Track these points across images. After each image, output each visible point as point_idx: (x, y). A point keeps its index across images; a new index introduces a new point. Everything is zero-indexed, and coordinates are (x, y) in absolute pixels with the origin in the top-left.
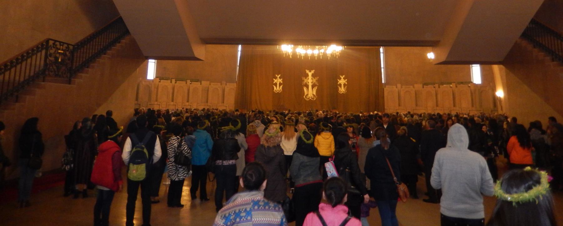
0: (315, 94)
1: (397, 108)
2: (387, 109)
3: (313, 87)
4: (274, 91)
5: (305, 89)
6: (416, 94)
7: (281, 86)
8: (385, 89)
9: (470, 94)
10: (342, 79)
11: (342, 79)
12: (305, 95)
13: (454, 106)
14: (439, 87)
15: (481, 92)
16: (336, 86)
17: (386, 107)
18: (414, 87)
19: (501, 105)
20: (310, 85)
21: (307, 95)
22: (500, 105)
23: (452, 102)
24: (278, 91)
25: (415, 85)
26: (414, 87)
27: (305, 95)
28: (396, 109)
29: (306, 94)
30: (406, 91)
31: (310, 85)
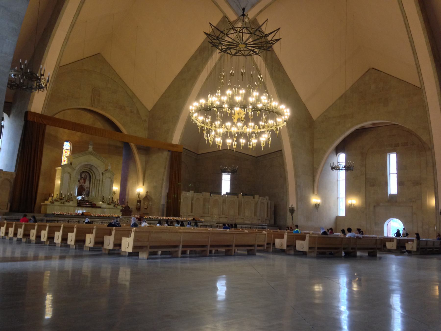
13: (239, 214)
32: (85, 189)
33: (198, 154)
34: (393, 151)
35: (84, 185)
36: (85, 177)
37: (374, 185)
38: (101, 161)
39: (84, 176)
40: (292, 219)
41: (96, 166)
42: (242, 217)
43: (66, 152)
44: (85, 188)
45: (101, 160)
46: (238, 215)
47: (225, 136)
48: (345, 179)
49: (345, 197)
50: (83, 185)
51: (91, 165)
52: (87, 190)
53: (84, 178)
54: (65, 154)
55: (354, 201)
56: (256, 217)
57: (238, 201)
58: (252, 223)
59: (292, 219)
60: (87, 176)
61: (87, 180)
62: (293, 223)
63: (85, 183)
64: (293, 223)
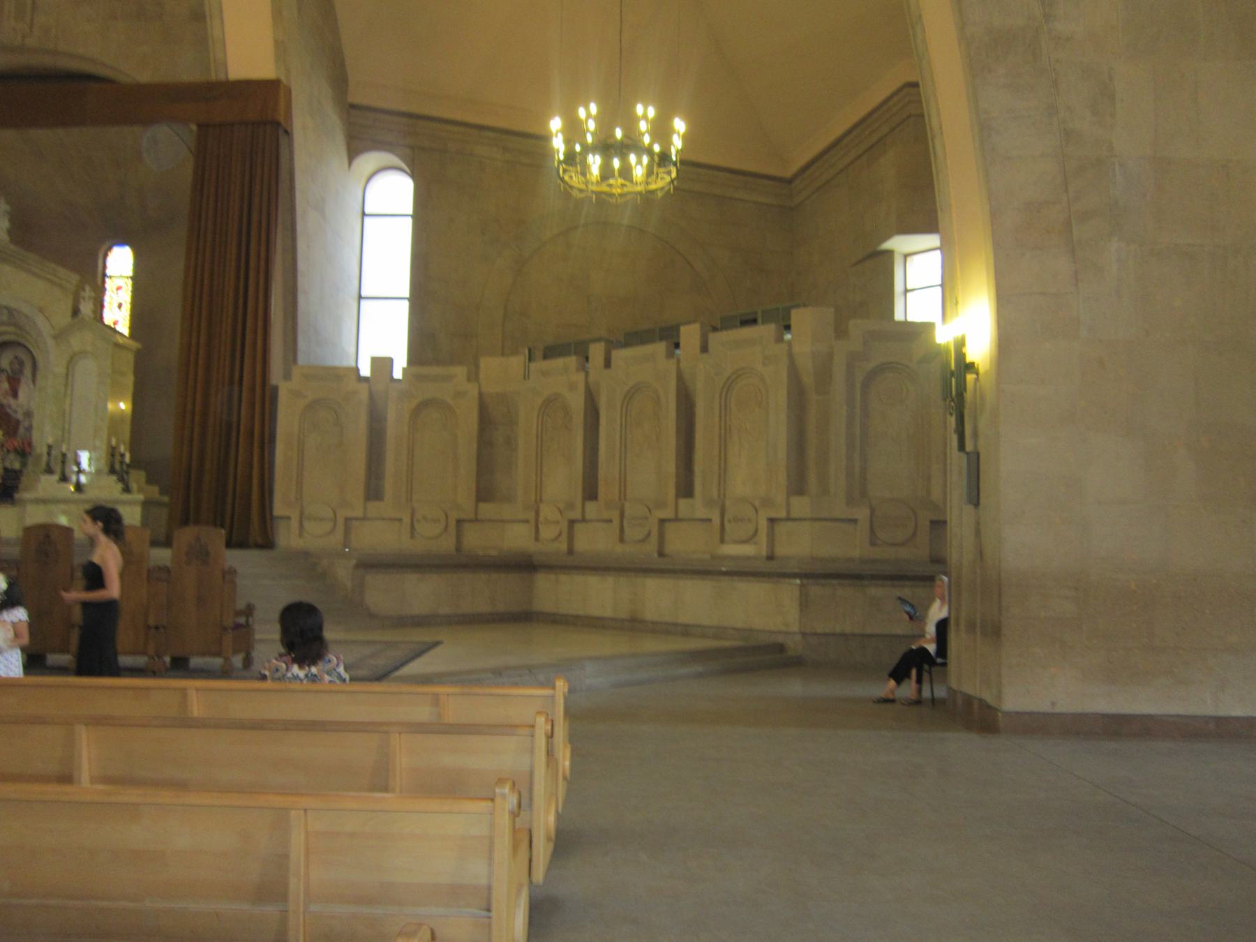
1: (350, 514)
2: (288, 518)
6: (485, 421)
9: (779, 398)
13: (686, 488)
14: (608, 364)
15: (872, 376)
17: (279, 509)
18: (473, 376)
19: (969, 447)
22: (962, 447)
23: (671, 467)
25: (485, 362)
26: (473, 376)
28: (347, 520)
30: (425, 404)
32: (18, 422)
33: (790, 181)
35: (12, 401)
36: (17, 366)
38: (50, 281)
39: (11, 363)
41: (25, 309)
42: (701, 512)
43: (119, 288)
44: (20, 416)
45: (49, 276)
46: (672, 492)
50: (10, 406)
51: (6, 308)
52: (26, 424)
53: (11, 374)
54: (114, 296)
56: (801, 506)
57: (673, 384)
58: (771, 557)
60: (21, 363)
61: (23, 380)
63: (15, 394)
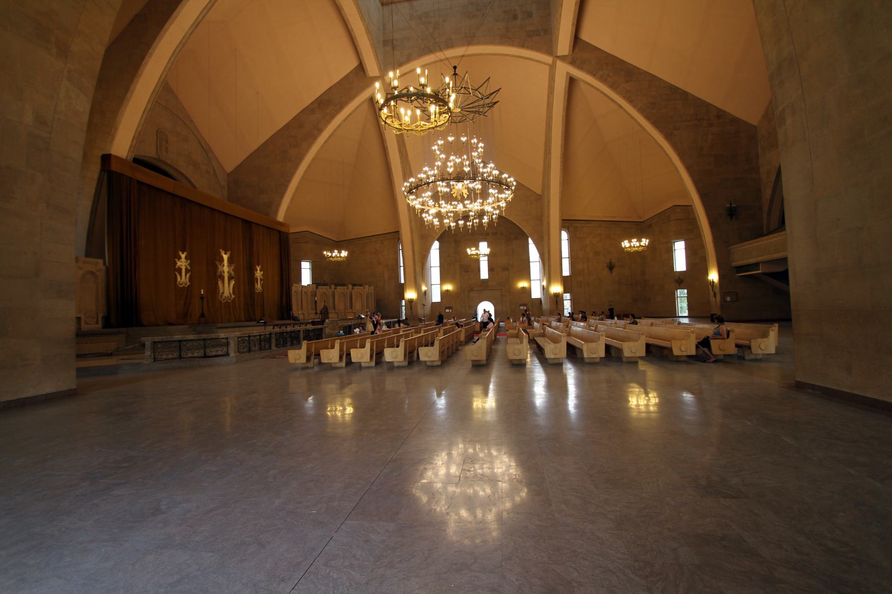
0: (231, 291)
3: (230, 278)
4: (177, 283)
5: (220, 283)
7: (188, 275)
8: (293, 288)
10: (258, 271)
11: (258, 271)
12: (220, 293)
16: (252, 280)
20: (226, 275)
21: (223, 293)
24: (184, 284)
27: (220, 293)
29: (221, 292)
31: (226, 275)
34: (679, 239)
37: (467, 272)
40: (411, 309)
47: (439, 215)
48: (439, 265)
49: (439, 283)
55: (449, 287)
59: (411, 309)
62: (412, 313)
64: (412, 313)
